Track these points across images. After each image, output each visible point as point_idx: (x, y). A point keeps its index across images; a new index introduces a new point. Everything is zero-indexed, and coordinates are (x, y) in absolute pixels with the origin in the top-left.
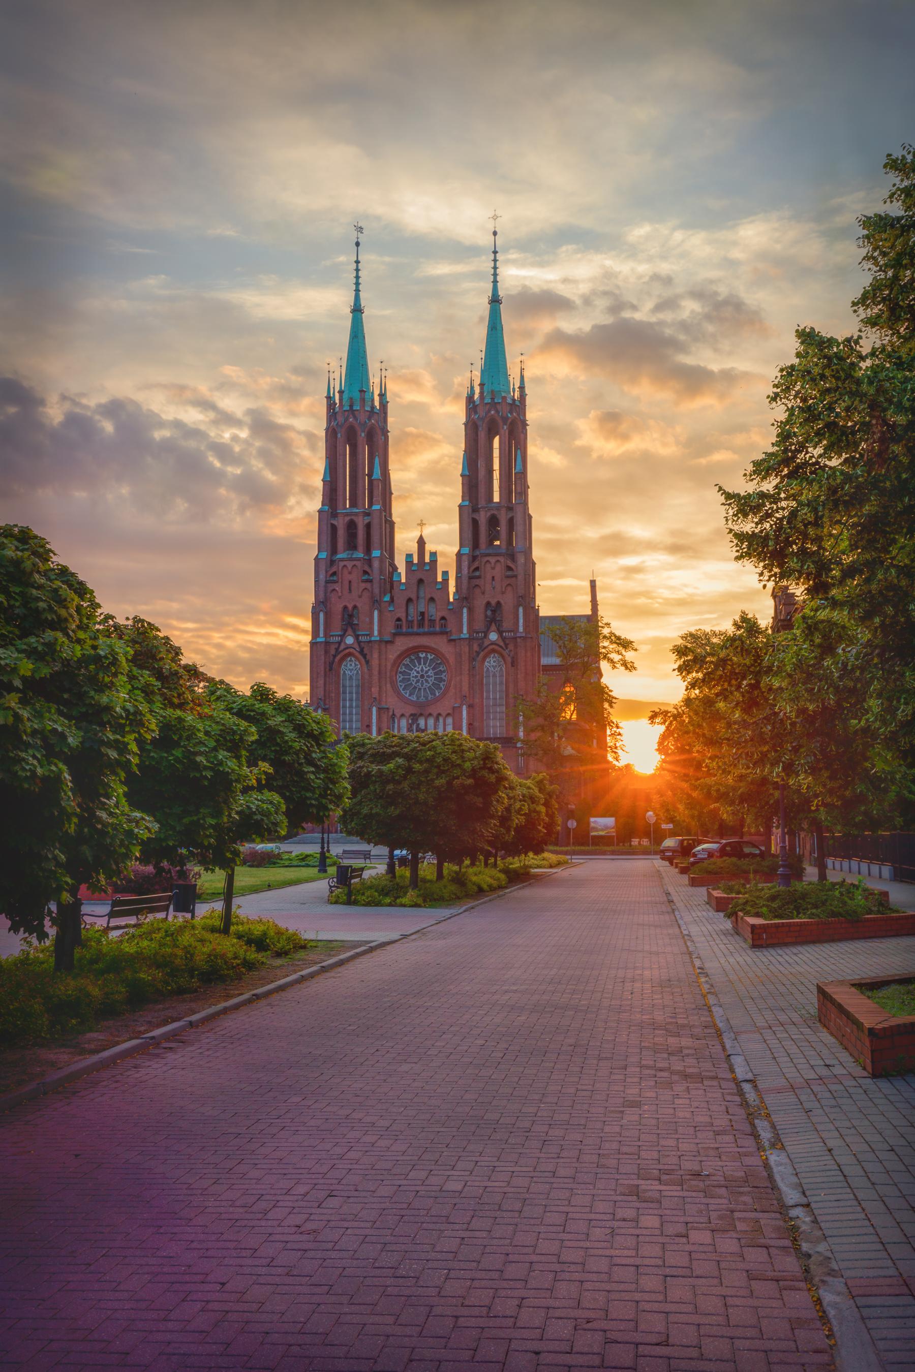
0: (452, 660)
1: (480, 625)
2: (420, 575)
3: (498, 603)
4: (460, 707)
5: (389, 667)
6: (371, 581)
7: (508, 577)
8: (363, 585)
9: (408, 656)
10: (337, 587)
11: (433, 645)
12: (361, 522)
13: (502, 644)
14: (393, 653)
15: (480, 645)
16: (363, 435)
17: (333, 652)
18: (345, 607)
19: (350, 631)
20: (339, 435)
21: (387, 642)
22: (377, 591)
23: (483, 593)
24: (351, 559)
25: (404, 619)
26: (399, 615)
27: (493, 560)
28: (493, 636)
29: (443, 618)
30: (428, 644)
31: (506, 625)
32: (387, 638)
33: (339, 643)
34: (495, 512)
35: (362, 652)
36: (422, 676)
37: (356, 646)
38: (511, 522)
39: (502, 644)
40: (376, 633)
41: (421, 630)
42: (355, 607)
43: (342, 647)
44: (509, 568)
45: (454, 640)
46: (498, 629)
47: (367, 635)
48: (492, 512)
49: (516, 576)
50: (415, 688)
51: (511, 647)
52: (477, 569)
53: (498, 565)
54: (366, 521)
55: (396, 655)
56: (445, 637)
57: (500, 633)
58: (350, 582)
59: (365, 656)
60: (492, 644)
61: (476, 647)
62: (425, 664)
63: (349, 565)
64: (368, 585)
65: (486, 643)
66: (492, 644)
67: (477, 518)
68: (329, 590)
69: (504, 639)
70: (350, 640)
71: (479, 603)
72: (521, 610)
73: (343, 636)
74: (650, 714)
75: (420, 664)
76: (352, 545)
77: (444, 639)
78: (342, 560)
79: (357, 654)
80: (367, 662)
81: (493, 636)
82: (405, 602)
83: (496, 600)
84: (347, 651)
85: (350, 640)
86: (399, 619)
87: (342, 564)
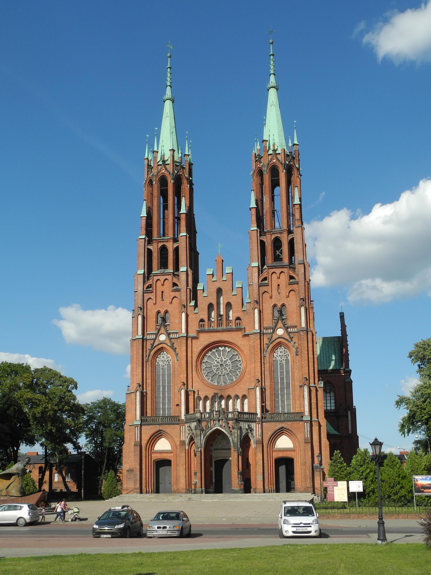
1: (268, 322)
2: (218, 285)
3: (283, 305)
4: (254, 389)
5: (195, 359)
6: (178, 290)
7: (290, 284)
8: (173, 294)
9: (211, 350)
10: (152, 296)
11: (230, 340)
13: (287, 337)
14: (197, 346)
15: (270, 339)
16: (172, 181)
17: (149, 347)
18: (159, 312)
19: (163, 330)
20: (154, 183)
21: (193, 338)
22: (184, 298)
23: (271, 297)
24: (163, 274)
25: (206, 320)
26: (202, 317)
27: (278, 271)
28: (280, 332)
29: (238, 319)
30: (226, 339)
31: (289, 323)
32: (192, 333)
33: (154, 340)
34: (279, 235)
35: (172, 346)
36: (221, 365)
37: (168, 342)
38: (291, 243)
39: (287, 337)
40: (184, 331)
41: (220, 328)
42: (166, 312)
43: (156, 344)
44: (291, 277)
45: (247, 335)
46: (284, 325)
47: (177, 333)
48: (276, 235)
49: (297, 283)
50: (215, 374)
51: (295, 339)
52: (265, 279)
53: (282, 274)
54: (175, 245)
55: (200, 348)
56: (240, 333)
57: (286, 329)
58: (163, 292)
59: (175, 350)
60: (278, 338)
61: (266, 341)
62: (223, 356)
63: (162, 278)
64: (177, 294)
65: (274, 338)
66: (278, 338)
67: (265, 240)
68: (146, 299)
69: (289, 333)
70: (162, 338)
71: (267, 306)
72: (303, 309)
73: (157, 335)
74: (398, 399)
75: (220, 356)
76: (164, 264)
77: (240, 334)
78: (156, 275)
79: (168, 348)
80: (177, 355)
81: (280, 332)
82: (207, 307)
83: (281, 303)
84: (160, 346)
85: (162, 338)
86: (202, 320)
87: (156, 278)
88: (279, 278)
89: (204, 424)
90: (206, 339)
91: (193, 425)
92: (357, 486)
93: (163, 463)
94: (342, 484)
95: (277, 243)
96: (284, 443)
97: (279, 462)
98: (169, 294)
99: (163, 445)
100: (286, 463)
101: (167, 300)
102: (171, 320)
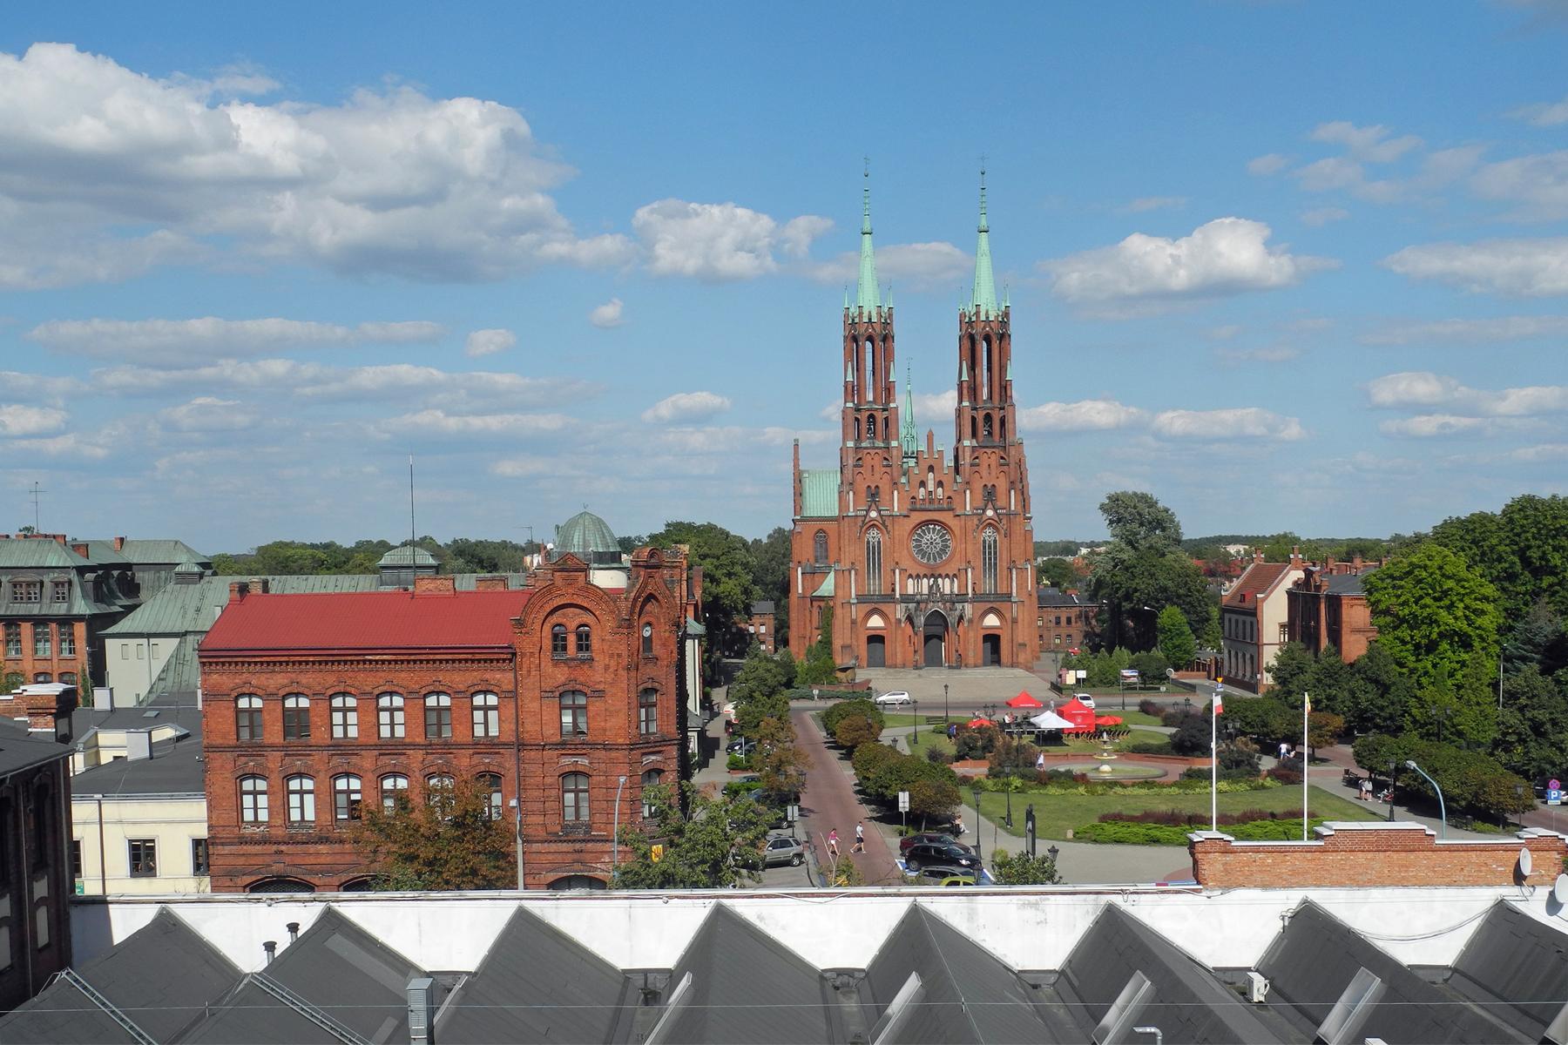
0: (957, 532)
12: (880, 416)
28: (990, 513)
31: (999, 504)
38: (1003, 422)
57: (995, 510)
70: (873, 514)
73: (868, 511)
81: (990, 513)
88: (990, 459)
89: (922, 606)
90: (917, 517)
91: (912, 606)
92: (1082, 674)
93: (876, 639)
94: (1072, 673)
95: (988, 418)
96: (992, 621)
97: (987, 638)
98: (879, 470)
99: (876, 622)
100: (992, 640)
101: (877, 476)
102: (884, 496)
